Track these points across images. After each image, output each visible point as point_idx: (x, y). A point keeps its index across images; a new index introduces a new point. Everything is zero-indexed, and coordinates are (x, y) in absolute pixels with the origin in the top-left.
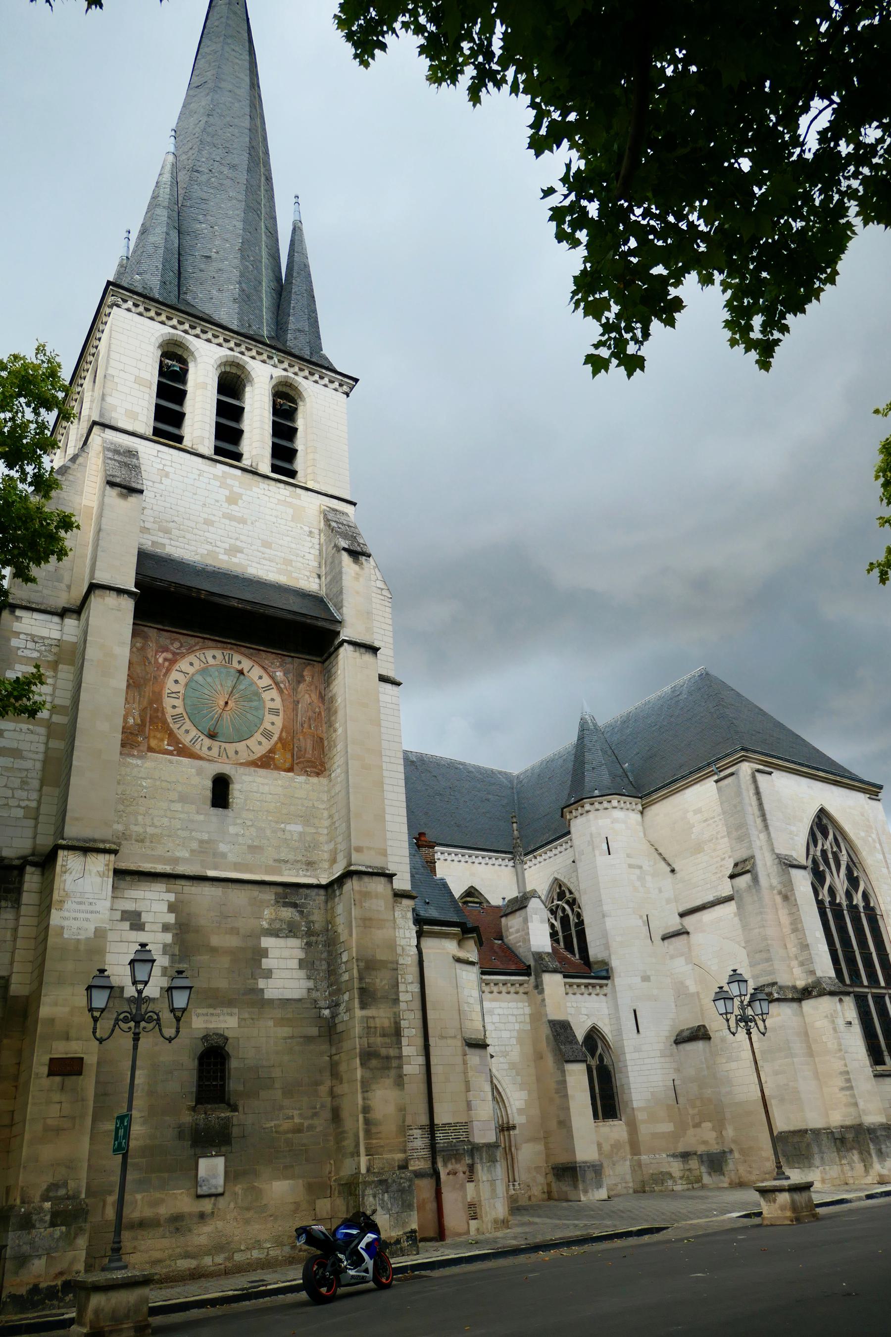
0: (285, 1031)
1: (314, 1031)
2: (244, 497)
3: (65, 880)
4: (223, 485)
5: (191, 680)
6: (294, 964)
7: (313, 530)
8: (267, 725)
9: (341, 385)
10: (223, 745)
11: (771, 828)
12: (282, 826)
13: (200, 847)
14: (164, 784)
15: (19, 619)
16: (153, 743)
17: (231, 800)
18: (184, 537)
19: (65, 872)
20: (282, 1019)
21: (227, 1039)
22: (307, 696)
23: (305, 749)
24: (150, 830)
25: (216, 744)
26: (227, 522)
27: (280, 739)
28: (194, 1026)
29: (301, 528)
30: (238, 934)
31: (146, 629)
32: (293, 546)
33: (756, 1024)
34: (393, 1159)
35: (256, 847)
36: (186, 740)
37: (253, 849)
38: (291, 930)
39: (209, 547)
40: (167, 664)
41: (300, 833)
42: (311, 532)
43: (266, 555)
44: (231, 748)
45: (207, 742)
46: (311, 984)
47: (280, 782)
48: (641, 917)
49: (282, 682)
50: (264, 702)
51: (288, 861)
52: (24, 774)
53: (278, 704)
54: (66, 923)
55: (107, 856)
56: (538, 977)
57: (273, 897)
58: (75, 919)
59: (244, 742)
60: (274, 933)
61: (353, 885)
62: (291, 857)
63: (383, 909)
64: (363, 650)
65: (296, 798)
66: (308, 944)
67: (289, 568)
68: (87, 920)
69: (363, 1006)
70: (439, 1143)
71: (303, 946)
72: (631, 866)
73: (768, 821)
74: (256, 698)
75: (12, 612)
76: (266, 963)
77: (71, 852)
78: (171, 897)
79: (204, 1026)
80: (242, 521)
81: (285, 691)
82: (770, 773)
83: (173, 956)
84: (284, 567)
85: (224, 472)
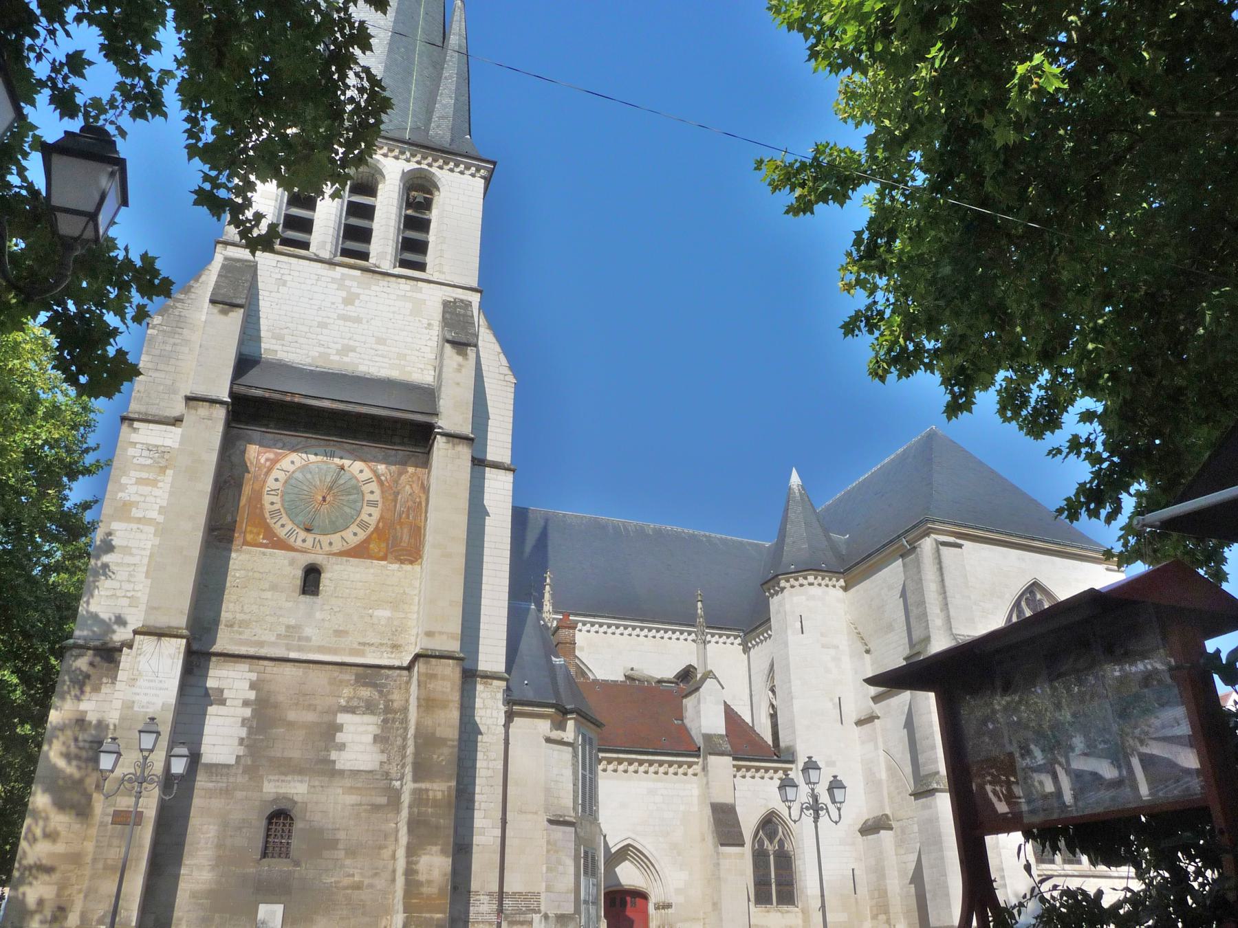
0: (352, 799)
1: (383, 800)
2: (361, 297)
3: (139, 662)
4: (341, 287)
5: (289, 478)
6: (370, 738)
7: (432, 322)
8: (364, 516)
9: (478, 170)
10: (318, 537)
11: (950, 606)
12: (371, 611)
13: (286, 631)
14: (257, 575)
15: (135, 430)
16: (249, 537)
17: (321, 588)
18: (296, 342)
19: (140, 655)
20: (351, 787)
21: (296, 803)
22: (408, 487)
23: (401, 538)
24: (240, 616)
25: (310, 538)
26: (341, 322)
27: (377, 528)
28: (264, 790)
29: (419, 321)
30: (315, 710)
31: (250, 432)
32: (409, 340)
33: (828, 812)
34: (432, 919)
35: (341, 631)
36: (282, 533)
37: (339, 633)
38: (370, 708)
39: (322, 350)
40: (268, 464)
41: (389, 618)
42: (429, 324)
43: (380, 353)
44: (325, 540)
45: (303, 534)
46: (384, 758)
47: (372, 571)
48: (832, 700)
49: (383, 475)
50: (363, 495)
51: (372, 644)
52: (132, 568)
53: (377, 496)
54: (137, 698)
55: (179, 640)
56: (705, 759)
57: (353, 677)
58: (146, 694)
59: (338, 535)
60: (350, 710)
61: (419, 667)
62: (375, 640)
63: (449, 690)
64: (456, 440)
65: (389, 585)
66: (385, 721)
67: (403, 362)
68: (156, 695)
69: (416, 779)
70: (507, 910)
71: (379, 723)
72: (824, 646)
73: (949, 599)
74: (355, 491)
75: (131, 426)
76: (340, 737)
77: (146, 637)
78: (254, 676)
79: (274, 790)
80: (358, 320)
81: (385, 483)
82: (960, 546)
83: (250, 729)
84: (397, 362)
85: (343, 274)
